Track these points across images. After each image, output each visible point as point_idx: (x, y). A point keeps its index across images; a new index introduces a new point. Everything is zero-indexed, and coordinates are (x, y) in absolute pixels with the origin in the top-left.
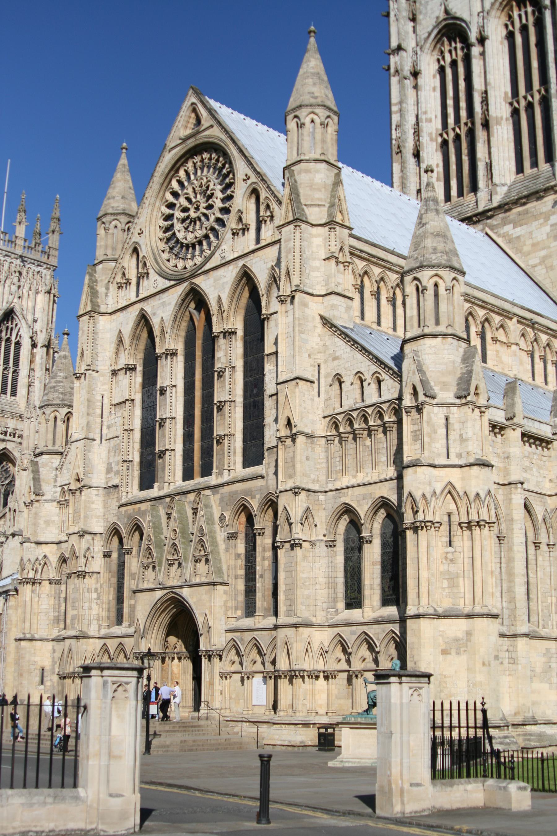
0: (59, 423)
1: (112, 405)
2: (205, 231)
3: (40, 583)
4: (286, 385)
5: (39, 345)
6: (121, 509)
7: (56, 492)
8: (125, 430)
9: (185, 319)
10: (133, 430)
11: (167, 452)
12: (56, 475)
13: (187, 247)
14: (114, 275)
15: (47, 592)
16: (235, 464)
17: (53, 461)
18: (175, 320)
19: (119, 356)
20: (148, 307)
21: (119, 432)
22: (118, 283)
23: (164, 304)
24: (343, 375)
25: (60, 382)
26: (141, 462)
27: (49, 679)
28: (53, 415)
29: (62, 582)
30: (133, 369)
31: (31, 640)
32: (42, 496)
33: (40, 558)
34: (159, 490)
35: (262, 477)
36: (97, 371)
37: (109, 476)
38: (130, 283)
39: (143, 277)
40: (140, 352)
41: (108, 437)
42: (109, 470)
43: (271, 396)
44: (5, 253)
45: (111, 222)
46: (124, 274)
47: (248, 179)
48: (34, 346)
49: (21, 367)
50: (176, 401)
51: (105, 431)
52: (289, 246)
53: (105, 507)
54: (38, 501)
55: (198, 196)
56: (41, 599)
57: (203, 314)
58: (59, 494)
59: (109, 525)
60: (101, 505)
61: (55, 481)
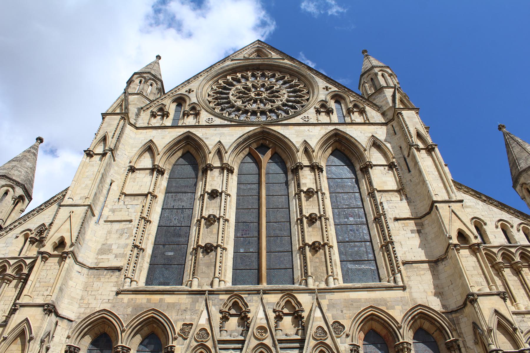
0: (9, 198)
1: (123, 193)
2: (270, 107)
4: (450, 204)
6: (120, 296)
8: (142, 218)
9: (244, 151)
10: (150, 222)
11: (219, 249)
13: (246, 112)
14: (148, 107)
16: (337, 275)
18: (236, 148)
19: (141, 159)
20: (199, 133)
21: (135, 217)
22: (153, 112)
23: (222, 134)
24: (482, 218)
26: (153, 256)
28: (6, 188)
30: (161, 172)
34: (199, 286)
35: (404, 288)
36: (114, 160)
37: (103, 257)
38: (168, 117)
39: (188, 116)
40: (170, 164)
41: (109, 219)
42: (105, 250)
43: (396, 219)
45: (150, 79)
46: (161, 110)
47: (330, 88)
50: (230, 208)
51: (106, 213)
52: (414, 121)
53: (85, 289)
55: (258, 89)
57: (269, 153)
59: (89, 312)
60: (80, 287)
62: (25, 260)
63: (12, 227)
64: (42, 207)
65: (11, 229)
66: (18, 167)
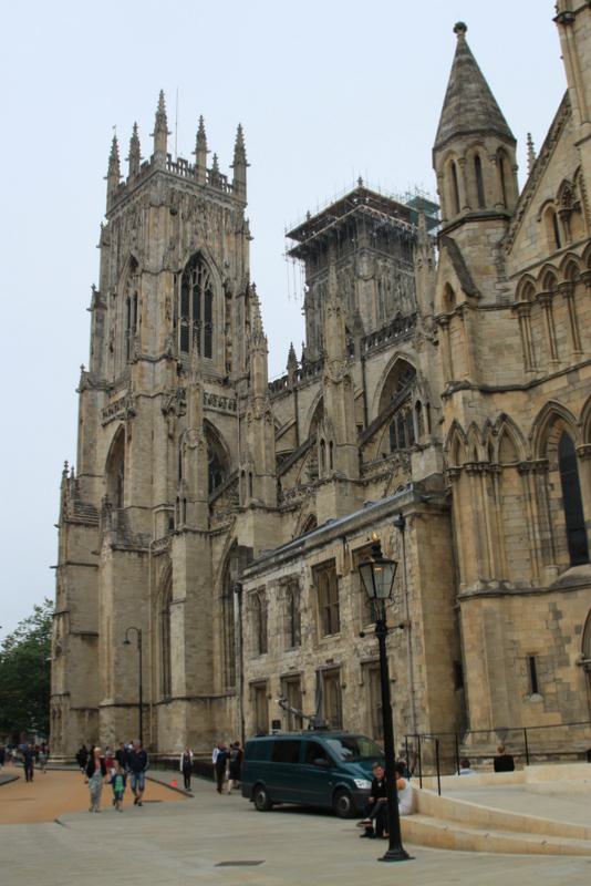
0: (485, 163)
3: (499, 473)
5: (234, 295)
7: (507, 290)
12: (501, 259)
15: (516, 492)
17: (489, 231)
25: (473, 98)
27: (550, 678)
28: (471, 152)
29: (551, 467)
31: (502, 594)
32: (479, 297)
33: (494, 421)
44: (186, 183)
48: (228, 296)
49: (214, 322)
54: (474, 308)
56: (506, 508)
58: (513, 292)
61: (501, 270)
62: (573, 251)
63: (521, 208)
64: (545, 153)
65: (522, 213)
66: (464, 105)
